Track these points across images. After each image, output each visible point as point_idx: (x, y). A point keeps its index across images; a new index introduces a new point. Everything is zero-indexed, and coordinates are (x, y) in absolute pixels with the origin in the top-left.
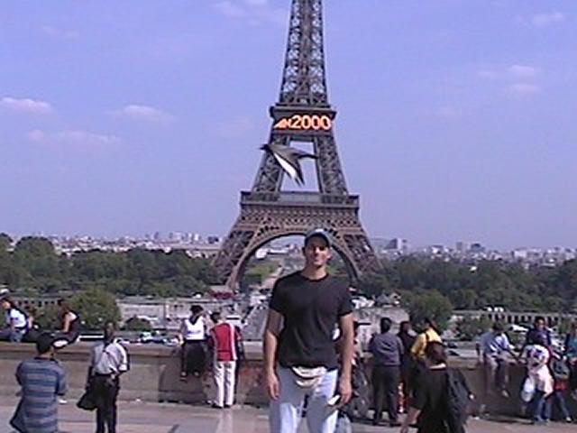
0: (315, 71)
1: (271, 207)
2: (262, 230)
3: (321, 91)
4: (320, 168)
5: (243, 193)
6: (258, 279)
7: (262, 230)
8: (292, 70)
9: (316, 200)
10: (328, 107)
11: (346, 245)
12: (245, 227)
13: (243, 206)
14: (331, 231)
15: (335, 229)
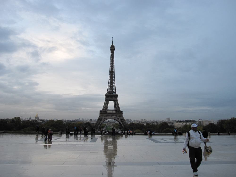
0: (114, 87)
1: (105, 114)
2: (104, 118)
3: (115, 91)
4: (115, 106)
5: (101, 111)
6: (103, 127)
7: (104, 118)
8: (109, 87)
9: (114, 112)
10: (116, 94)
11: (120, 121)
12: (101, 118)
13: (100, 113)
14: (117, 118)
15: (118, 118)
